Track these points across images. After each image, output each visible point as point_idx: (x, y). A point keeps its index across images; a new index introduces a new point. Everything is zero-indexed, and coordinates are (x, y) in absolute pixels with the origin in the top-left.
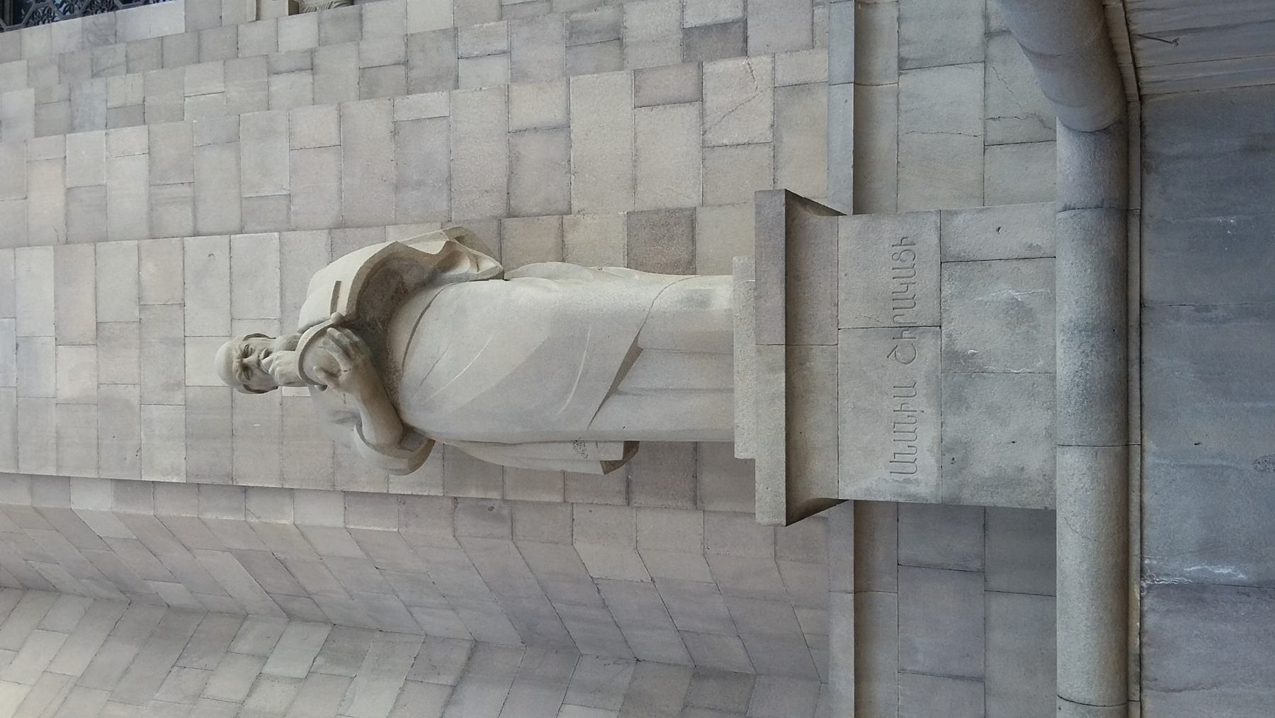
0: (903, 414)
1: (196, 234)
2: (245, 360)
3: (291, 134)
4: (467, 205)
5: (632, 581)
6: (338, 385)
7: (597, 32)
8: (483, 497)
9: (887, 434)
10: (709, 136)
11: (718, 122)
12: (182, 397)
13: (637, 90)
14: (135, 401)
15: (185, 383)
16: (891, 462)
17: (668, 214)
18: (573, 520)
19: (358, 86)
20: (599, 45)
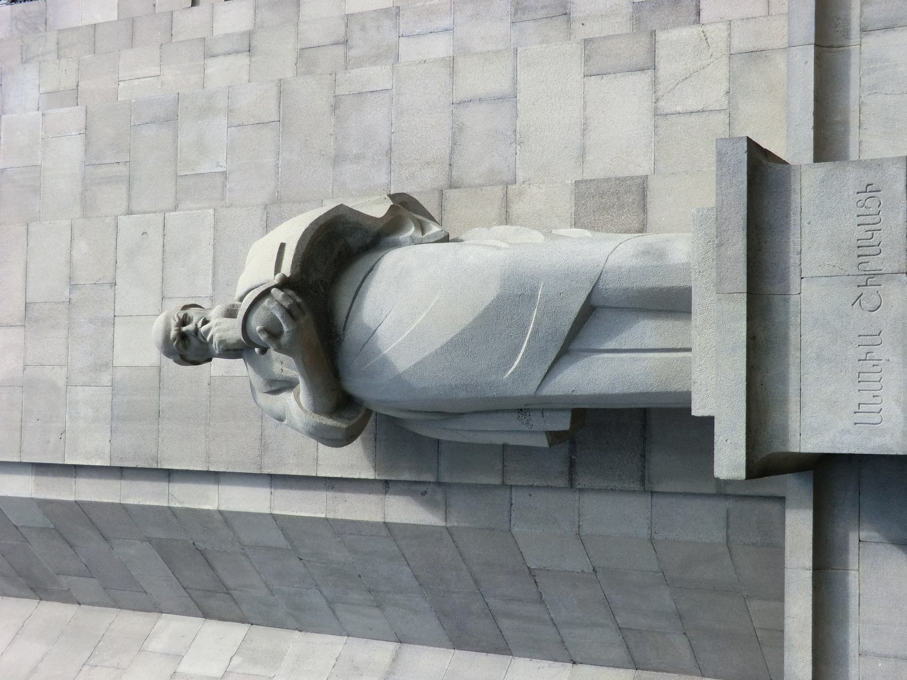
0: (868, 364)
1: (129, 212)
2: (184, 329)
3: (230, 111)
4: (407, 178)
5: (572, 572)
6: (280, 349)
7: (543, 8)
8: (417, 480)
9: (852, 384)
10: (661, 103)
11: (671, 90)
12: (109, 377)
13: (587, 59)
14: (61, 383)
15: (113, 364)
16: (855, 413)
17: (618, 182)
18: (512, 504)
19: (295, 67)
20: (545, 21)
